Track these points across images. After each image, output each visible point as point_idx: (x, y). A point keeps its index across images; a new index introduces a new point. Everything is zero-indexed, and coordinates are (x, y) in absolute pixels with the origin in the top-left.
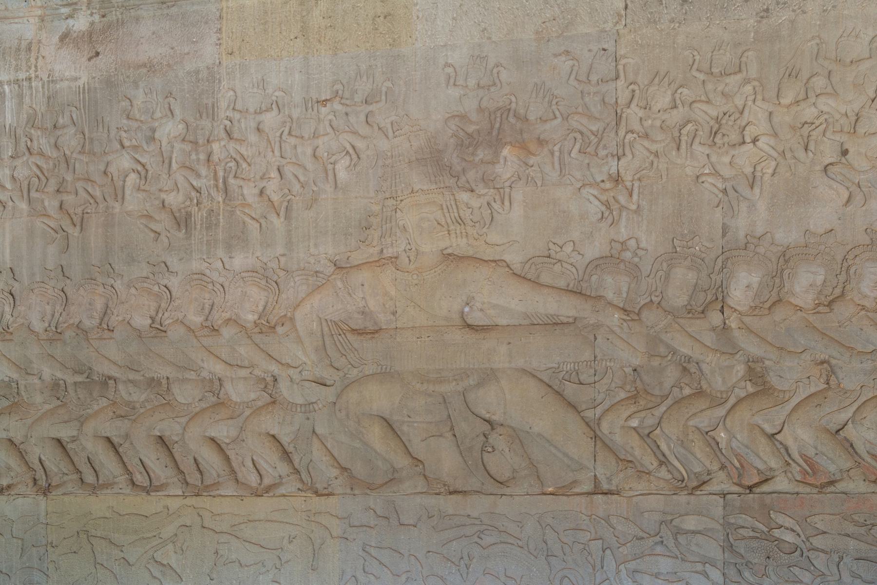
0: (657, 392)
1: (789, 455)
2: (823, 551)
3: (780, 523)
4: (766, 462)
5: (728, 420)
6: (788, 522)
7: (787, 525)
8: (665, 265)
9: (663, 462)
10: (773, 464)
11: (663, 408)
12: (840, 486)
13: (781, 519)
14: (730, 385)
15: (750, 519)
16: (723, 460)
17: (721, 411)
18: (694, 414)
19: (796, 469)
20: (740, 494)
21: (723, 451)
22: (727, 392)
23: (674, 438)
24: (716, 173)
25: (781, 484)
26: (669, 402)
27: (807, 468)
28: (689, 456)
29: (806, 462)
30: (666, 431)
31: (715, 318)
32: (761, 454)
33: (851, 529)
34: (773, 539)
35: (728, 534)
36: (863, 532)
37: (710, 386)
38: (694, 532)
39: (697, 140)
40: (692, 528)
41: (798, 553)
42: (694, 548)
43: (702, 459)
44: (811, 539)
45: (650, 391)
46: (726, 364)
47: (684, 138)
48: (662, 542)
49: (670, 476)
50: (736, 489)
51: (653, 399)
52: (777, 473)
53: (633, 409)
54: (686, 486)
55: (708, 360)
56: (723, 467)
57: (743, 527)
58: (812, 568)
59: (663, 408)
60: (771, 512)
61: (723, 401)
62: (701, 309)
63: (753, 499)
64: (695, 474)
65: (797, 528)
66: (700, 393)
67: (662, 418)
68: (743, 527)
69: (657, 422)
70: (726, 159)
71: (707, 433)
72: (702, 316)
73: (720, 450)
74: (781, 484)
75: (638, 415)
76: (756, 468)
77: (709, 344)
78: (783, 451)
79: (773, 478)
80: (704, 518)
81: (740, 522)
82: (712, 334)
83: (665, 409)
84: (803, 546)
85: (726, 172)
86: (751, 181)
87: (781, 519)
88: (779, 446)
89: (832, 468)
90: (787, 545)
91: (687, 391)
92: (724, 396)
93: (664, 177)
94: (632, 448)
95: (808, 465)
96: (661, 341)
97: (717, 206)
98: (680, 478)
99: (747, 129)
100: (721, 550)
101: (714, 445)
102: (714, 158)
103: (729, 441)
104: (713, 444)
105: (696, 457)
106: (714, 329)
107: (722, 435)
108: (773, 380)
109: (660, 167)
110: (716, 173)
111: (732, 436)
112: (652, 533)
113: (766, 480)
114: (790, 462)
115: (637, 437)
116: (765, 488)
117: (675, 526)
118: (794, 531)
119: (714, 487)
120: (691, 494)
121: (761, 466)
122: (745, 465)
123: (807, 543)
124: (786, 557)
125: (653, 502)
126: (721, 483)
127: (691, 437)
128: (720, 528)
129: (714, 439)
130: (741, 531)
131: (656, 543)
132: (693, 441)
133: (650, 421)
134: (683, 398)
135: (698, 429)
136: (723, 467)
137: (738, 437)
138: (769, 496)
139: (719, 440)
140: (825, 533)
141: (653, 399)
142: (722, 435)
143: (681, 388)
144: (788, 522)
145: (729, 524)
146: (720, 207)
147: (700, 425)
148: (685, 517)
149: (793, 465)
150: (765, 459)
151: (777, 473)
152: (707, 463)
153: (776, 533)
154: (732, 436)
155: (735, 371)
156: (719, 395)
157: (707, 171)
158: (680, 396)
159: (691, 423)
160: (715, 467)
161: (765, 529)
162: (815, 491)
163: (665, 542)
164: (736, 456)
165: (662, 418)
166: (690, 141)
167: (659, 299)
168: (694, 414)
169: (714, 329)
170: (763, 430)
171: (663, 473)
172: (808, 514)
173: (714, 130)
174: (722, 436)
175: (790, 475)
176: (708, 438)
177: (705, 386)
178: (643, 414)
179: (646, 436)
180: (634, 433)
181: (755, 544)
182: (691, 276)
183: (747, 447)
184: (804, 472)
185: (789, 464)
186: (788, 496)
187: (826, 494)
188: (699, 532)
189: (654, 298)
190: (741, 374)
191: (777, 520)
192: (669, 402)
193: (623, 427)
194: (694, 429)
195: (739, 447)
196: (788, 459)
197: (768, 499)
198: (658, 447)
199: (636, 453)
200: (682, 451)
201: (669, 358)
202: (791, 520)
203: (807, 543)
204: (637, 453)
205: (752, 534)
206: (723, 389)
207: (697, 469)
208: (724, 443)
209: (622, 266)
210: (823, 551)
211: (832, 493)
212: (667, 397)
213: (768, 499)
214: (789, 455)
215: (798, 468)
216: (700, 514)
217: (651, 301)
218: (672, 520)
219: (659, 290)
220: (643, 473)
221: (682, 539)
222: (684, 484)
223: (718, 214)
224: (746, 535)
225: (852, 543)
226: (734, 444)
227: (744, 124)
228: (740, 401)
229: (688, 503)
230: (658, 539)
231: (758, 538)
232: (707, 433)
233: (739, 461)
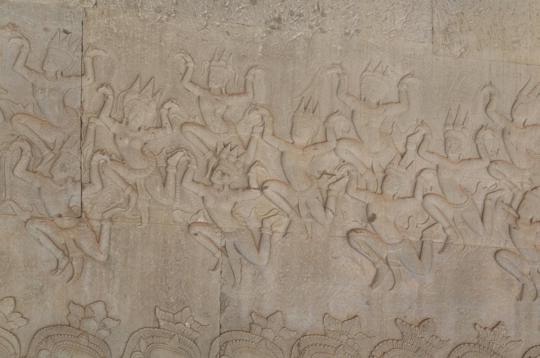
209: (83, 340)
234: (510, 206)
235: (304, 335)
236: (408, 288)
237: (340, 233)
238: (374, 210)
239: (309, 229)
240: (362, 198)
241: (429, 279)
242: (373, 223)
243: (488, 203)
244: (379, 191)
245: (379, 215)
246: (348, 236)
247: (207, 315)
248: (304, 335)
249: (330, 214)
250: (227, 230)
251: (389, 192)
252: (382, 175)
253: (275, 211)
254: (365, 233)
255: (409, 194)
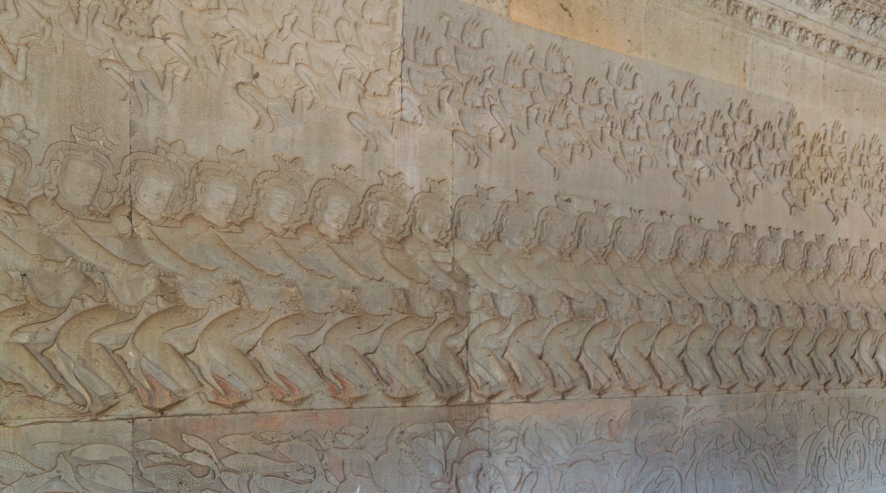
0: (53, 303)
1: (202, 375)
2: (235, 471)
3: (193, 446)
4: (178, 383)
5: (137, 337)
6: (200, 444)
7: (199, 447)
8: (61, 154)
9: (61, 384)
10: (185, 385)
11: (60, 322)
12: (251, 406)
13: (193, 442)
14: (139, 299)
15: (161, 444)
16: (132, 382)
17: (129, 328)
18: (98, 331)
19: (208, 390)
20: (150, 418)
21: (132, 371)
22: (136, 307)
23: (74, 357)
24: (122, 63)
25: (194, 405)
26: (68, 315)
27: (219, 389)
28: (93, 377)
29: (218, 382)
30: (64, 348)
31: (122, 224)
32: (173, 375)
33: (261, 447)
34: (185, 463)
35: (137, 462)
36: (270, 449)
37: (117, 300)
38: (98, 463)
39: (99, 19)
40: (96, 458)
41: (210, 475)
42: (98, 480)
43: (108, 381)
44: (223, 461)
45: (45, 302)
46: (135, 276)
47: (84, 12)
48: (60, 477)
49: (70, 401)
50: (147, 412)
51: (48, 311)
52: (189, 394)
53: (21, 321)
54: (89, 411)
55: (114, 270)
56: (132, 390)
57: (154, 453)
58: (224, 489)
59: (60, 322)
60: (184, 435)
61: (131, 316)
62: (105, 212)
63: (165, 422)
64: (101, 397)
65: (210, 450)
66: (105, 307)
67: (59, 333)
68: (154, 453)
69: (53, 337)
70: (134, 50)
71: (114, 351)
72: (107, 220)
73: (129, 370)
74: (194, 405)
75: (27, 329)
76: (167, 389)
77: (115, 253)
78: (196, 371)
79: (185, 399)
80: (110, 446)
81: (151, 448)
82: (119, 241)
83: (63, 323)
84: (215, 468)
85: (134, 64)
86: (162, 80)
87: (193, 442)
88: (192, 367)
89: (243, 388)
90: (200, 469)
91: (90, 304)
92: (133, 311)
93: (60, 51)
94: (21, 368)
95: (220, 386)
96: (58, 244)
97: (124, 100)
98: (82, 403)
99: (157, 22)
100: (130, 480)
101: (121, 366)
102: (120, 44)
103: (139, 361)
104: (120, 363)
105: (100, 378)
106: (120, 237)
107: (131, 354)
108: (186, 296)
109: (54, 37)
110: (122, 63)
111: (142, 356)
112: (47, 467)
113: (179, 402)
114: (203, 382)
115: (26, 355)
116: (177, 410)
117: (75, 458)
118: (206, 453)
119: (122, 411)
120: (96, 420)
121: (173, 388)
122: (156, 386)
123: (220, 465)
124: (199, 480)
125: (47, 431)
126: (130, 406)
127: (94, 356)
128: (128, 455)
129: (122, 358)
130: (152, 457)
131: (52, 479)
132: (96, 360)
133: (44, 337)
134: (85, 311)
135: (103, 347)
136: (132, 390)
137: (148, 356)
138: (181, 418)
139: (127, 359)
140: (237, 453)
141: (48, 311)
142: (131, 354)
143: (83, 300)
144: (200, 444)
145: (139, 451)
146: (128, 101)
147: (106, 343)
148: (90, 447)
149: (207, 385)
150: (177, 380)
151: (189, 394)
152: (114, 386)
153: (189, 457)
154: (142, 356)
155: (144, 285)
156: (127, 310)
157: (112, 57)
158: (82, 309)
159: (94, 340)
160: (123, 389)
161: (177, 454)
162: (227, 411)
163: (63, 477)
164: (146, 377)
165: (59, 333)
166: (91, 17)
167: (54, 194)
168: (98, 331)
169: (120, 237)
170: (175, 350)
171: (61, 397)
172: (220, 435)
173: (119, 13)
174: (130, 354)
175: (202, 396)
176: (115, 357)
177: (111, 300)
178: (34, 328)
179: (39, 355)
180: (23, 351)
181: (166, 470)
182: (94, 173)
183: (158, 367)
184: (217, 393)
185: (201, 385)
186: (201, 417)
187: (237, 414)
188: (105, 463)
189: (48, 192)
190: (152, 288)
191: (190, 444)
192: (68, 315)
193: (7, 343)
194: (98, 347)
195: (149, 368)
196: (201, 380)
197: (180, 422)
198: (55, 366)
199: (26, 374)
200: (85, 371)
201: (67, 264)
202: (203, 442)
203: (220, 465)
204: (28, 374)
205: (163, 460)
206: (131, 304)
207: (103, 391)
208: (133, 363)
210: (235, 471)
211: (243, 413)
212: (65, 309)
213: (180, 422)
214: (202, 375)
215: (211, 389)
216: (104, 442)
217: (44, 195)
218: (72, 451)
219: (55, 183)
220: (35, 398)
221: (83, 472)
222: (86, 410)
223: (125, 109)
224: (157, 461)
225: (261, 461)
226: (144, 364)
227: (153, 15)
228: (151, 317)
229: (92, 431)
230: (54, 474)
231: (169, 463)
232: (114, 351)
233: (148, 382)
234: (360, 81)
235: (201, 161)
236: (284, 133)
237: (230, 84)
238: (257, 69)
239: (205, 77)
240: (249, 59)
241: (300, 128)
242: (257, 80)
243: (344, 76)
244: (262, 55)
245: (261, 74)
246: (237, 87)
247: (118, 137)
248: (201, 161)
249: (222, 68)
250: (134, 69)
251: (270, 57)
252: (263, 43)
253: (176, 59)
254: (251, 87)
255: (285, 61)
